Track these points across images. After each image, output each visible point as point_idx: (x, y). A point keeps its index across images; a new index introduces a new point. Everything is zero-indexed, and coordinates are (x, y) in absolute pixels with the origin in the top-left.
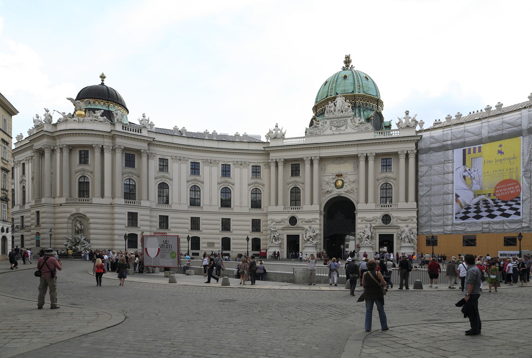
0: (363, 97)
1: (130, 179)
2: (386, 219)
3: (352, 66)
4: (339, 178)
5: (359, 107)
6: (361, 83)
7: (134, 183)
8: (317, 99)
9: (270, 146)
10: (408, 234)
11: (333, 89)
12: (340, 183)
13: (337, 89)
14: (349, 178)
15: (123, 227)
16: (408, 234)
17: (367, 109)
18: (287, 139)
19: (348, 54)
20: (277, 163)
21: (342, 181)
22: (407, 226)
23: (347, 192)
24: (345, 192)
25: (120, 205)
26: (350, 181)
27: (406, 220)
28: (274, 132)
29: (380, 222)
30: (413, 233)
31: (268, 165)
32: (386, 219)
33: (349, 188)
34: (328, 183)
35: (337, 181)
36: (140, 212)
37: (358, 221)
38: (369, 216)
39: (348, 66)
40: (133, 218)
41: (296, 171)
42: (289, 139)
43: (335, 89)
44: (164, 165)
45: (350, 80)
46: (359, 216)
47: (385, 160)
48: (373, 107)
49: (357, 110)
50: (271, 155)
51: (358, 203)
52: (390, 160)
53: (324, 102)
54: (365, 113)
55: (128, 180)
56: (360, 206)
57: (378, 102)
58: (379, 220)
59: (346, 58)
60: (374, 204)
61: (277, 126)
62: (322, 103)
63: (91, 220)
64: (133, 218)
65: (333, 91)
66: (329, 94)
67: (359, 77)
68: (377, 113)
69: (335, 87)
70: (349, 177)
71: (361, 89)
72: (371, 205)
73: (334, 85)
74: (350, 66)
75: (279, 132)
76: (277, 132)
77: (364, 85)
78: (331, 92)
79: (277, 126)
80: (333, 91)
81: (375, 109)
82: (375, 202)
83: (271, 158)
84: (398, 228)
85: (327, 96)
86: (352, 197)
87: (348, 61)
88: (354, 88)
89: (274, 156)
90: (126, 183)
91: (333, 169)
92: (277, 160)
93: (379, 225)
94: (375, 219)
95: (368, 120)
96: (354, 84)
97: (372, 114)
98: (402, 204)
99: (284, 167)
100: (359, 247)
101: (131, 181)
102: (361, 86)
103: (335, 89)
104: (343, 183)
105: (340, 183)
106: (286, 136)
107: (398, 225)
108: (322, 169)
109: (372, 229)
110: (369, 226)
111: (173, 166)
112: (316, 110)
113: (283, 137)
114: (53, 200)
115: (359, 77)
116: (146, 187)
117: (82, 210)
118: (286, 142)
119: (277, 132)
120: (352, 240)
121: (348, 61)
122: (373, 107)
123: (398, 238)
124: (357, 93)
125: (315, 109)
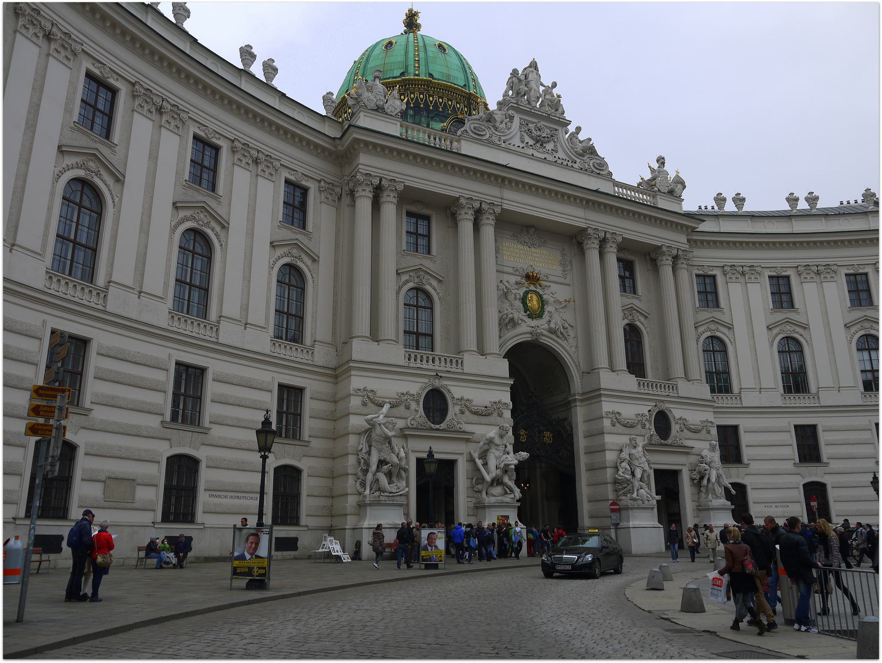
4: (532, 288)
11: (422, 62)
12: (534, 303)
14: (557, 292)
20: (378, 191)
21: (540, 296)
26: (557, 302)
33: (557, 321)
35: (527, 293)
43: (427, 65)
70: (554, 288)
80: (422, 68)
84: (686, 451)
85: (402, 74)
86: (568, 351)
92: (384, 182)
103: (427, 65)
104: (542, 302)
105: (534, 303)
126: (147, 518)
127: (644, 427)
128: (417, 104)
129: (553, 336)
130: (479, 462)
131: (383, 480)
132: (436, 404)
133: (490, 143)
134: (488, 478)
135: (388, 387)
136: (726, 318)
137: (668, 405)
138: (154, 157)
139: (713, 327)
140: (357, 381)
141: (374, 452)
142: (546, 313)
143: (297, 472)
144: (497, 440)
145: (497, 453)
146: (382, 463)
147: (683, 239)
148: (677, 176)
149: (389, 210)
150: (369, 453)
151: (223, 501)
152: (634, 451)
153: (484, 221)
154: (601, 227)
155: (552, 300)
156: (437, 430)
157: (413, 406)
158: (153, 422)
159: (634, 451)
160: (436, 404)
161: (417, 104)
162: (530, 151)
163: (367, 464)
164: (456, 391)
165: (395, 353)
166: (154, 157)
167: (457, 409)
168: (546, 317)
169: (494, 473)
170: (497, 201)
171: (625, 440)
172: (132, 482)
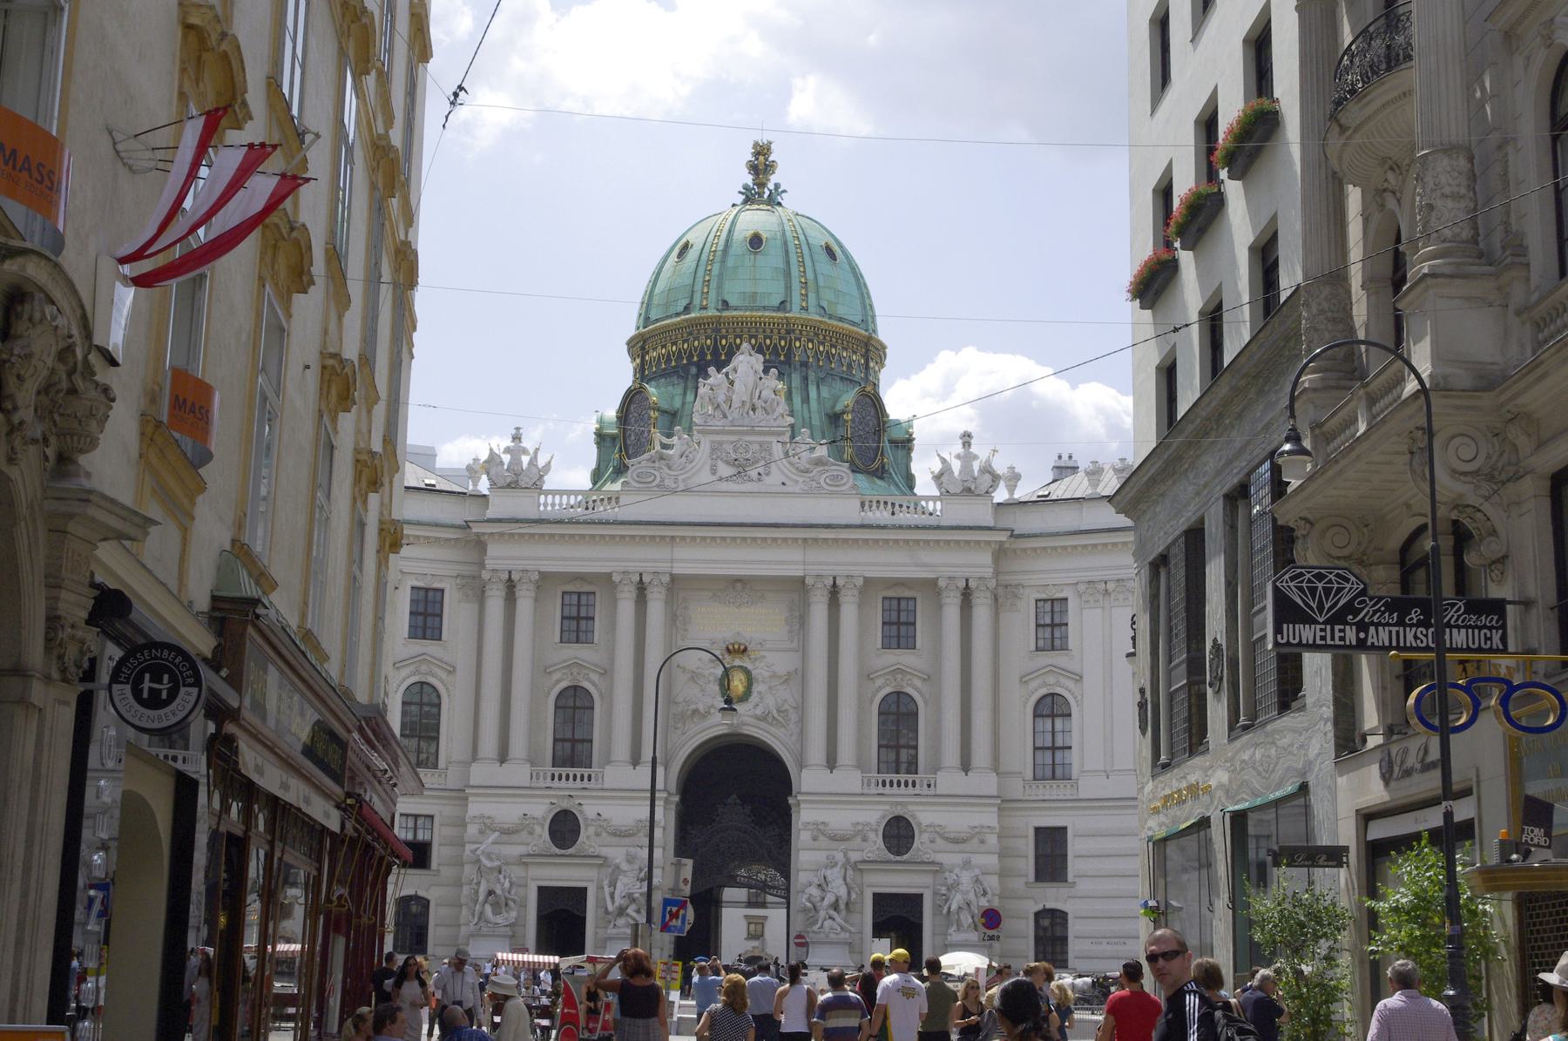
0: (817, 333)
2: (899, 834)
3: (777, 186)
4: (737, 662)
5: (805, 364)
6: (810, 275)
8: (647, 304)
9: (490, 514)
10: (971, 896)
11: (713, 285)
13: (727, 285)
14: (771, 663)
16: (971, 896)
17: (830, 374)
18: (554, 493)
19: (763, 138)
20: (511, 586)
21: (748, 673)
22: (967, 865)
23: (763, 718)
24: (757, 718)
26: (774, 676)
27: (964, 841)
28: (506, 458)
29: (875, 846)
30: (985, 893)
31: (477, 590)
32: (899, 834)
33: (770, 702)
34: (694, 677)
37: (801, 837)
38: (840, 818)
39: (762, 185)
41: (577, 624)
42: (561, 493)
43: (720, 287)
45: (771, 259)
46: (805, 816)
47: (895, 603)
48: (850, 366)
49: (796, 379)
50: (493, 550)
51: (801, 765)
52: (911, 603)
53: (677, 328)
54: (825, 392)
56: (809, 780)
57: (871, 351)
58: (872, 836)
59: (757, 154)
60: (858, 774)
61: (517, 438)
62: (665, 330)
65: (713, 295)
66: (697, 301)
67: (805, 247)
68: (864, 394)
69: (721, 275)
71: (812, 296)
72: (848, 779)
73: (716, 268)
74: (771, 186)
75: (525, 459)
76: (516, 461)
77: (821, 283)
78: (705, 295)
79: (517, 438)
80: (713, 295)
81: (858, 374)
82: (860, 765)
83: (490, 564)
84: (937, 869)
85: (687, 309)
86: (778, 740)
87: (761, 163)
88: (788, 288)
89: (501, 557)
91: (715, 624)
92: (515, 577)
93: (872, 857)
94: (860, 832)
95: (835, 418)
96: (788, 274)
97: (848, 398)
98: (951, 780)
99: (536, 600)
100: (805, 945)
102: (811, 285)
103: (720, 287)
105: (738, 684)
106: (550, 482)
107: (939, 858)
108: (674, 619)
109: (850, 872)
110: (840, 857)
112: (644, 351)
113: (537, 486)
115: (805, 247)
118: (548, 505)
119: (516, 461)
120: (776, 905)
121: (761, 163)
122: (850, 366)
123: (937, 908)
124: (795, 313)
125: (639, 346)
127: (865, 839)
128: (702, 355)
129: (763, 725)
130: (607, 890)
131: (488, 909)
132: (564, 828)
133: (664, 490)
134: (610, 908)
135: (508, 812)
136: (1074, 666)
137: (911, 808)
139: (1051, 679)
140: (475, 808)
141: (483, 882)
142: (755, 694)
143: (425, 903)
144: (624, 866)
145: (625, 880)
146: (491, 893)
147: (986, 558)
148: (988, 461)
149: (525, 605)
150: (479, 883)
152: (828, 872)
153: (649, 596)
154: (829, 571)
155: (767, 674)
156: (570, 856)
157: (538, 829)
159: (828, 872)
160: (564, 828)
161: (702, 355)
162: (724, 486)
163: (477, 892)
164: (588, 810)
165: (517, 772)
167: (591, 830)
168: (754, 698)
169: (618, 901)
170: (663, 567)
171: (821, 857)
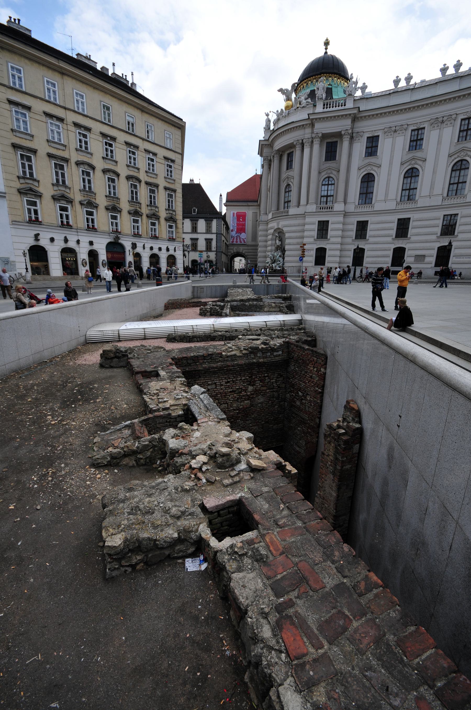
1: (329, 177)
7: (333, 182)
15: (312, 240)
25: (312, 214)
36: (331, 219)
40: (323, 228)
44: (372, 146)
55: (327, 179)
63: (287, 235)
64: (323, 228)
90: (324, 183)
101: (331, 179)
111: (384, 145)
114: (266, 216)
116: (344, 184)
117: (282, 223)
126: (429, 266)
138: (439, 142)
151: (461, 259)
158: (434, 237)
166: (439, 142)
172: (424, 256)
